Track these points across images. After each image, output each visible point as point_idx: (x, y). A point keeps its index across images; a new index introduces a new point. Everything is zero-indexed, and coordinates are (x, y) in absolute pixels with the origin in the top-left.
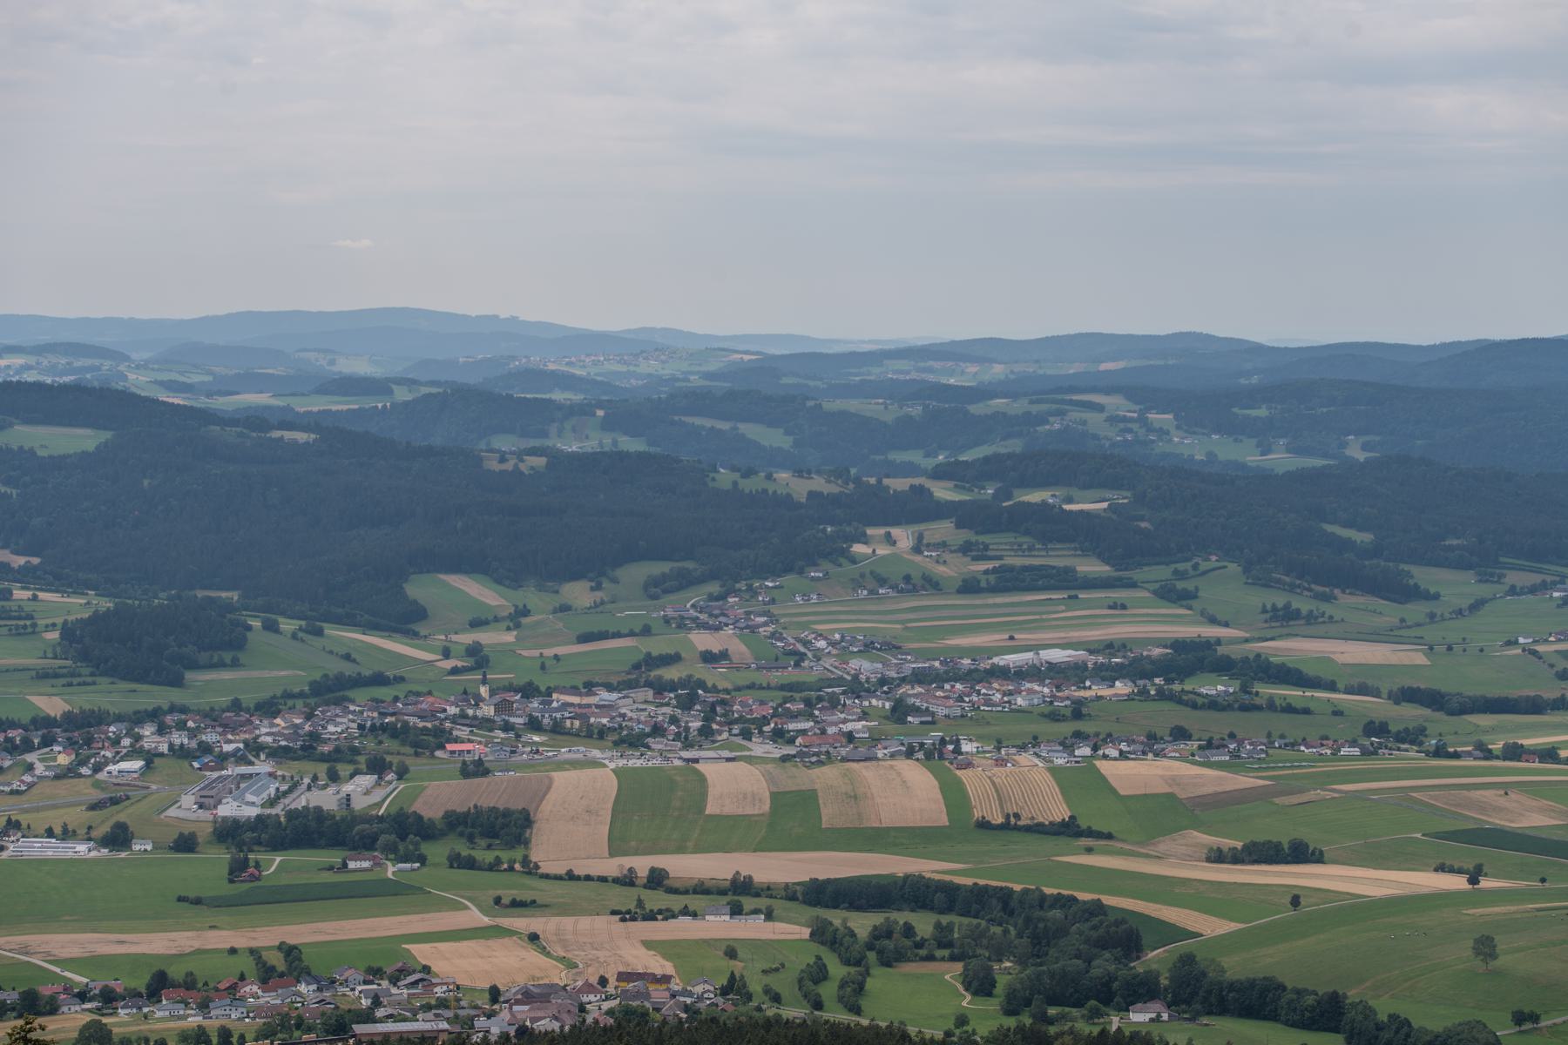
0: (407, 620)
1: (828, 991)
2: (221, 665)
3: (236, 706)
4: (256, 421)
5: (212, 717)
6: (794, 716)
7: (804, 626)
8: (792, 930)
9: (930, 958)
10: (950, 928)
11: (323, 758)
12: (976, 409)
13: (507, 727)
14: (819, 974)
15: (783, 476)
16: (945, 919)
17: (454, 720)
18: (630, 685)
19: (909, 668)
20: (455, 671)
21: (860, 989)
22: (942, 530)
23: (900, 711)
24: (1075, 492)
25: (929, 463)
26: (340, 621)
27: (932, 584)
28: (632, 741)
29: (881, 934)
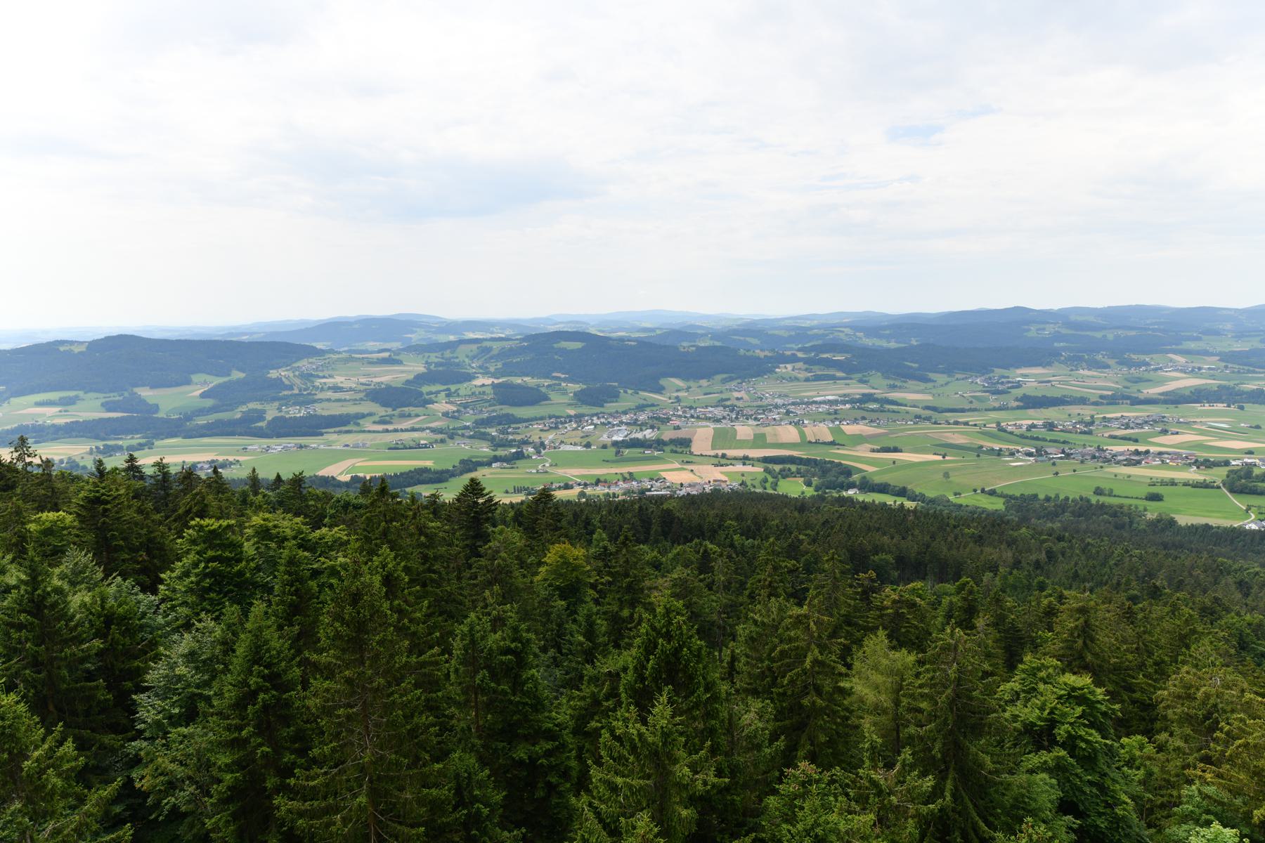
0: (660, 390)
1: (768, 485)
2: (613, 402)
3: (617, 412)
4: (621, 339)
5: (611, 415)
6: (760, 414)
7: (763, 390)
8: (759, 469)
9: (795, 477)
10: (800, 469)
11: (639, 425)
12: (809, 333)
13: (685, 417)
14: (765, 481)
15: (757, 351)
16: (799, 467)
17: (672, 415)
18: (717, 406)
19: (790, 402)
20: (672, 403)
21: (776, 484)
22: (800, 365)
23: (788, 413)
24: (836, 354)
25: (797, 347)
26: (645, 390)
27: (797, 379)
28: (718, 421)
29: (781, 470)
